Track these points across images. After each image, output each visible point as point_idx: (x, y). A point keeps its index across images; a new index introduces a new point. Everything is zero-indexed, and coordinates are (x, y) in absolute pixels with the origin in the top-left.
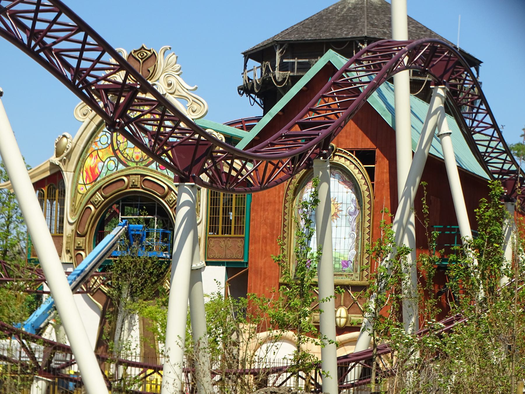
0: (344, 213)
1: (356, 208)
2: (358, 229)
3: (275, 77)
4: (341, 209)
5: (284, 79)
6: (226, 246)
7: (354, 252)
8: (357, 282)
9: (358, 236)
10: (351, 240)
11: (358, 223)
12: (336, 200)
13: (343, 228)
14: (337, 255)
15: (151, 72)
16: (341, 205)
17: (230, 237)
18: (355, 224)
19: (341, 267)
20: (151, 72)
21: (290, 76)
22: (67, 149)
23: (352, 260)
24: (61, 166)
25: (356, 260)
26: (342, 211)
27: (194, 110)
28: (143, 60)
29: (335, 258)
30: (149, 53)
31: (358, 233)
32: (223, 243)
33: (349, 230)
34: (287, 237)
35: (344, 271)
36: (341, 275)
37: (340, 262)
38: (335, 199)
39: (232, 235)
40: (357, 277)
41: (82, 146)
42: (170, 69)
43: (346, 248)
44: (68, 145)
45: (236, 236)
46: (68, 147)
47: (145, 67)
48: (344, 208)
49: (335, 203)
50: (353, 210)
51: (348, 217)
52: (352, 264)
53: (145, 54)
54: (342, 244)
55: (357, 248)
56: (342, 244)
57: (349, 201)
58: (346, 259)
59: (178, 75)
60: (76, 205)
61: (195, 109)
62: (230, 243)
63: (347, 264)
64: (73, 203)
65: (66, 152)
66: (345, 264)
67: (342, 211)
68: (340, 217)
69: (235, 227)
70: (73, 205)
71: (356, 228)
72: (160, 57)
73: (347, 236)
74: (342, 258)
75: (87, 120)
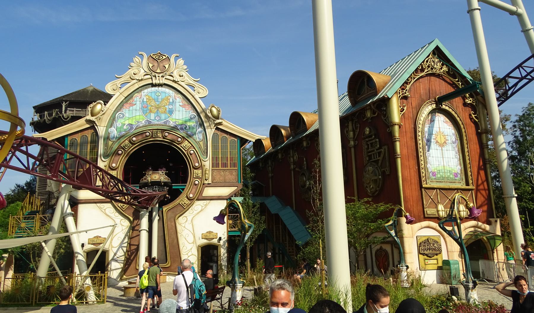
0: (450, 141)
1: (456, 139)
2: (459, 152)
3: (63, 116)
4: (447, 139)
5: (68, 117)
6: (225, 175)
7: (459, 167)
8: (464, 187)
9: (460, 157)
10: (456, 160)
11: (458, 149)
12: (444, 133)
13: (451, 152)
14: (451, 170)
15: (167, 68)
16: (447, 137)
17: (227, 169)
18: (457, 149)
19: (454, 177)
20: (167, 68)
21: (71, 116)
22: (103, 111)
23: (459, 172)
24: (96, 122)
25: (462, 173)
26: (448, 140)
27: (199, 92)
28: (160, 60)
29: (450, 171)
30: (164, 57)
31: (459, 155)
32: (222, 173)
33: (454, 152)
34: (423, 156)
35: (456, 180)
36: (455, 182)
37: (453, 174)
38: (443, 133)
39: (229, 168)
40: (464, 184)
41: (114, 110)
42: (181, 67)
43: (455, 164)
44: (103, 108)
45: (231, 168)
46: (103, 110)
47: (161, 65)
48: (449, 138)
49: (444, 135)
50: (454, 140)
51: (452, 144)
52: (459, 175)
53: (161, 58)
54: (452, 162)
55: (461, 165)
56: (452, 162)
57: (451, 135)
58: (456, 172)
59: (186, 71)
60: (108, 149)
61: (200, 92)
62: (227, 173)
63: (457, 175)
64: (106, 148)
65: (102, 113)
66: (456, 175)
67: (448, 140)
68: (448, 144)
69: (230, 163)
70: (106, 149)
71: (458, 152)
72: (172, 59)
73: (454, 157)
74: (453, 171)
75: (118, 94)
